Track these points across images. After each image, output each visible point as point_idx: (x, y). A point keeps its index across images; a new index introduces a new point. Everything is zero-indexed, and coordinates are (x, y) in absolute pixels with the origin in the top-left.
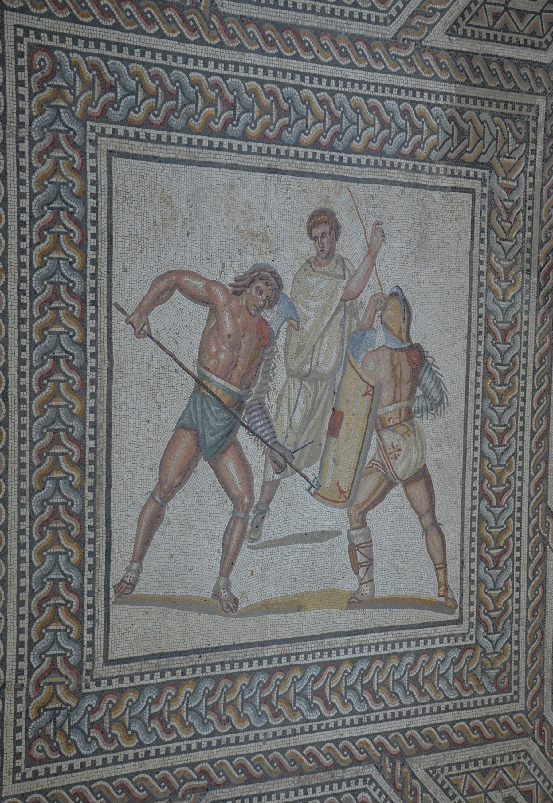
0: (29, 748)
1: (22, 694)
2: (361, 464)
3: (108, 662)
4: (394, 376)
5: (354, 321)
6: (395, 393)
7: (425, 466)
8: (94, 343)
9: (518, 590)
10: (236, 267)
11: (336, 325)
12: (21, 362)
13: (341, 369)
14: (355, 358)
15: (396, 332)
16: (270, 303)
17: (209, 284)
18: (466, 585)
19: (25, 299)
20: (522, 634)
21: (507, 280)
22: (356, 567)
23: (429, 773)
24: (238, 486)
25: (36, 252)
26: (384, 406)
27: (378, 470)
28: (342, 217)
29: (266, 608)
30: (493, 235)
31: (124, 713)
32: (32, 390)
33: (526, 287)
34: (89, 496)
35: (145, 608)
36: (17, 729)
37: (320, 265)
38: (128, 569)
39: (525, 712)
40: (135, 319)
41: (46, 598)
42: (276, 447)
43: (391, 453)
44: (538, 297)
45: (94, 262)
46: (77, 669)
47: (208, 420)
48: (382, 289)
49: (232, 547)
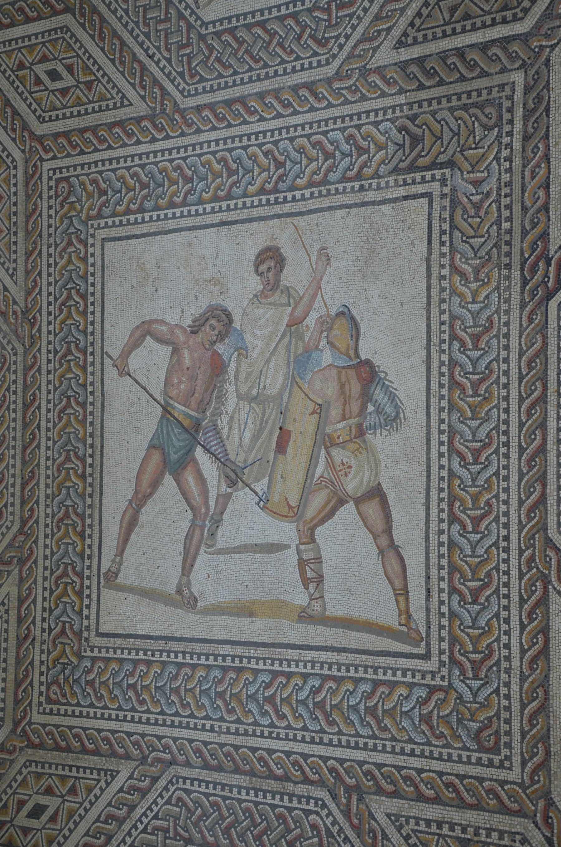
0: (48, 689)
1: (45, 647)
2: (309, 481)
3: (99, 635)
4: (343, 393)
5: (300, 344)
6: (344, 410)
7: (379, 484)
8: (92, 384)
9: (508, 633)
10: (193, 310)
12: (49, 402)
13: (288, 390)
14: (301, 378)
15: (343, 350)
16: (221, 337)
17: (172, 328)
18: (434, 618)
19: (51, 356)
20: (515, 688)
21: (477, 280)
22: (306, 582)
23: (390, 819)
25: (58, 322)
26: (333, 424)
27: (327, 487)
28: (286, 251)
30: (457, 234)
31: (109, 678)
32: (54, 422)
33: (504, 284)
34: (89, 501)
35: (125, 594)
36: (41, 674)
37: (266, 297)
38: (113, 561)
39: (521, 785)
40: (119, 362)
42: (228, 463)
43: (340, 471)
44: (522, 293)
45: (92, 323)
46: (78, 634)
47: (172, 440)
48: (328, 311)
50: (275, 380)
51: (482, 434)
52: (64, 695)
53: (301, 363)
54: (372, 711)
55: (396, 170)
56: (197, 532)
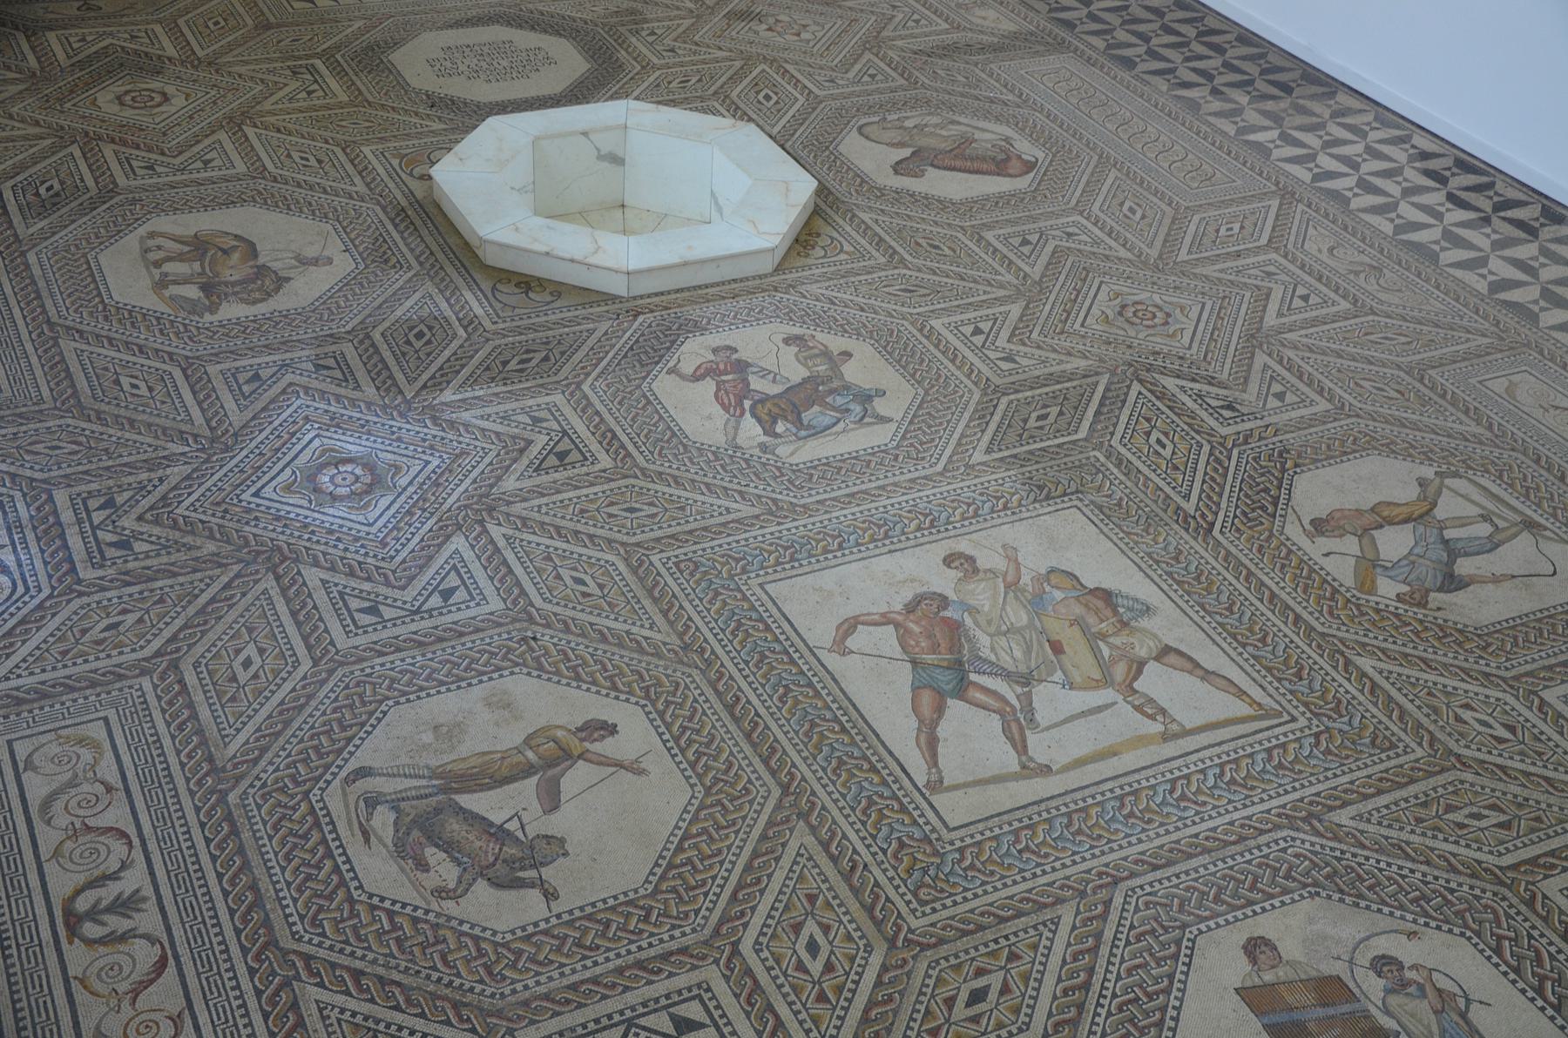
16: (945, 608)
17: (883, 615)
18: (1279, 698)
22: (1152, 717)
28: (969, 551)
29: (1080, 763)
38: (929, 774)
41: (868, 807)
49: (1017, 737)
50: (1018, 616)
52: (942, 891)
53: (1037, 603)
56: (1014, 726)
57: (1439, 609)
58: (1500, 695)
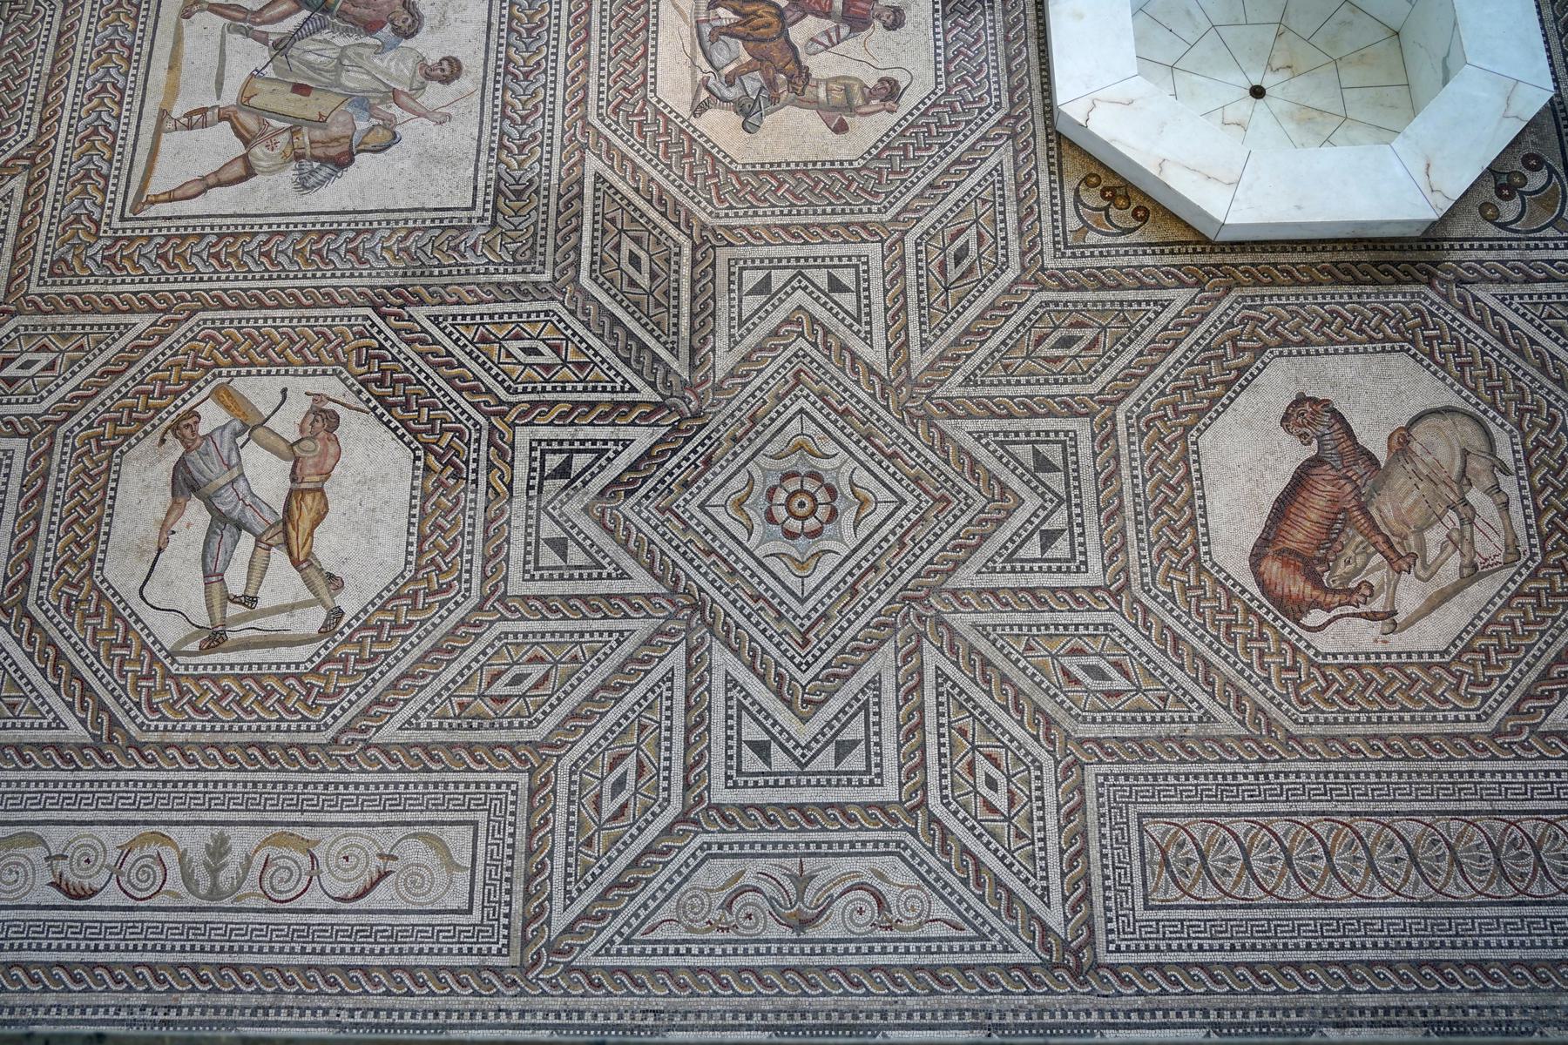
11: (376, 85)
16: (396, 30)
18: (150, 224)
20: (93, 288)
22: (189, 115)
24: (268, 14)
28: (455, 85)
29: (178, 40)
50: (353, 80)
51: (282, 259)
53: (363, 103)
54: (87, 175)
55: (500, 178)
57: (163, 441)
58: (45, 404)
